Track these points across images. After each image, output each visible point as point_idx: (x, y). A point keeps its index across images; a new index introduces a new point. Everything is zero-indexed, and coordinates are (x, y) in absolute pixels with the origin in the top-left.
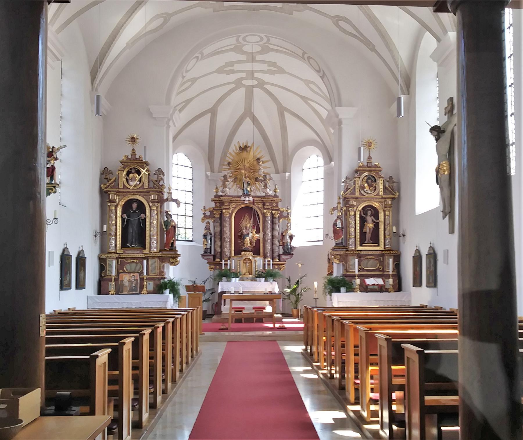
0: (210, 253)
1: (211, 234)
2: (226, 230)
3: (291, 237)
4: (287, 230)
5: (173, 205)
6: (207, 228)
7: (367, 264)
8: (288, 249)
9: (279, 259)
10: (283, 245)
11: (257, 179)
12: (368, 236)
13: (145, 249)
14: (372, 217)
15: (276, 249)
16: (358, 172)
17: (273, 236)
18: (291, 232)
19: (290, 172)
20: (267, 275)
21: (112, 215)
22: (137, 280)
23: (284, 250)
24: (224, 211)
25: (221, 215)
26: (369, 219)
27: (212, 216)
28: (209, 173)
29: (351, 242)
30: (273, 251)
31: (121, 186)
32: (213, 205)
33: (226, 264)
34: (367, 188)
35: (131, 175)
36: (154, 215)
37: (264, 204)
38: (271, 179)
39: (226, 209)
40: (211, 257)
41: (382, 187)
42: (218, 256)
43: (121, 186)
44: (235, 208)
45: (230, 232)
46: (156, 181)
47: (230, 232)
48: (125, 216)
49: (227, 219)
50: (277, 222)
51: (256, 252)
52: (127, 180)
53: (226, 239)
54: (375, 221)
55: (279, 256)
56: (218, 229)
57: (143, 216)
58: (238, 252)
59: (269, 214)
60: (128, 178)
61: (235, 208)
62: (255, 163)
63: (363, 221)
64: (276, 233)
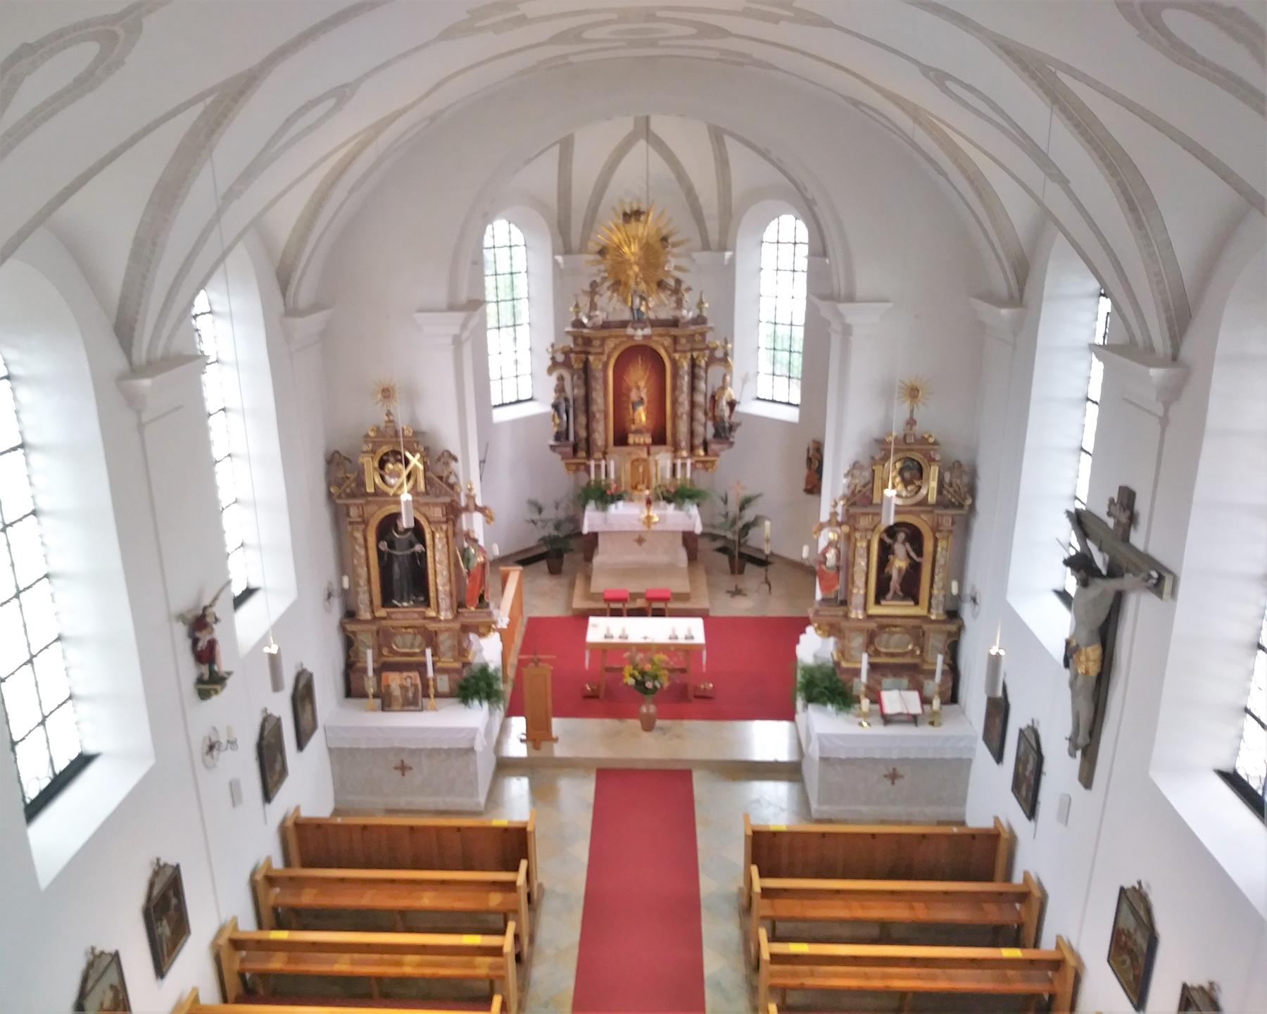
0: (567, 438)
1: (566, 400)
2: (597, 396)
3: (732, 404)
4: (723, 388)
5: (478, 518)
6: (560, 389)
8: (724, 428)
9: (706, 450)
10: (714, 418)
11: (661, 285)
12: (895, 583)
13: (428, 605)
14: (908, 545)
15: (699, 429)
16: (881, 449)
17: (693, 404)
18: (732, 392)
19: (734, 249)
20: (678, 495)
21: (357, 548)
22: (415, 686)
23: (716, 430)
24: (591, 358)
25: (586, 363)
27: (567, 364)
28: (560, 259)
29: (858, 592)
30: (692, 433)
31: (370, 489)
32: (569, 342)
33: (598, 467)
37: (675, 340)
38: (689, 289)
39: (596, 354)
40: (569, 450)
41: (934, 484)
42: (583, 445)
43: (370, 489)
45: (603, 401)
47: (603, 401)
48: (384, 546)
49: (599, 375)
50: (702, 373)
51: (659, 439)
52: (383, 478)
54: (913, 555)
55: (705, 445)
56: (580, 392)
58: (621, 439)
59: (685, 365)
61: (615, 348)
62: (658, 246)
63: (886, 552)
64: (700, 398)
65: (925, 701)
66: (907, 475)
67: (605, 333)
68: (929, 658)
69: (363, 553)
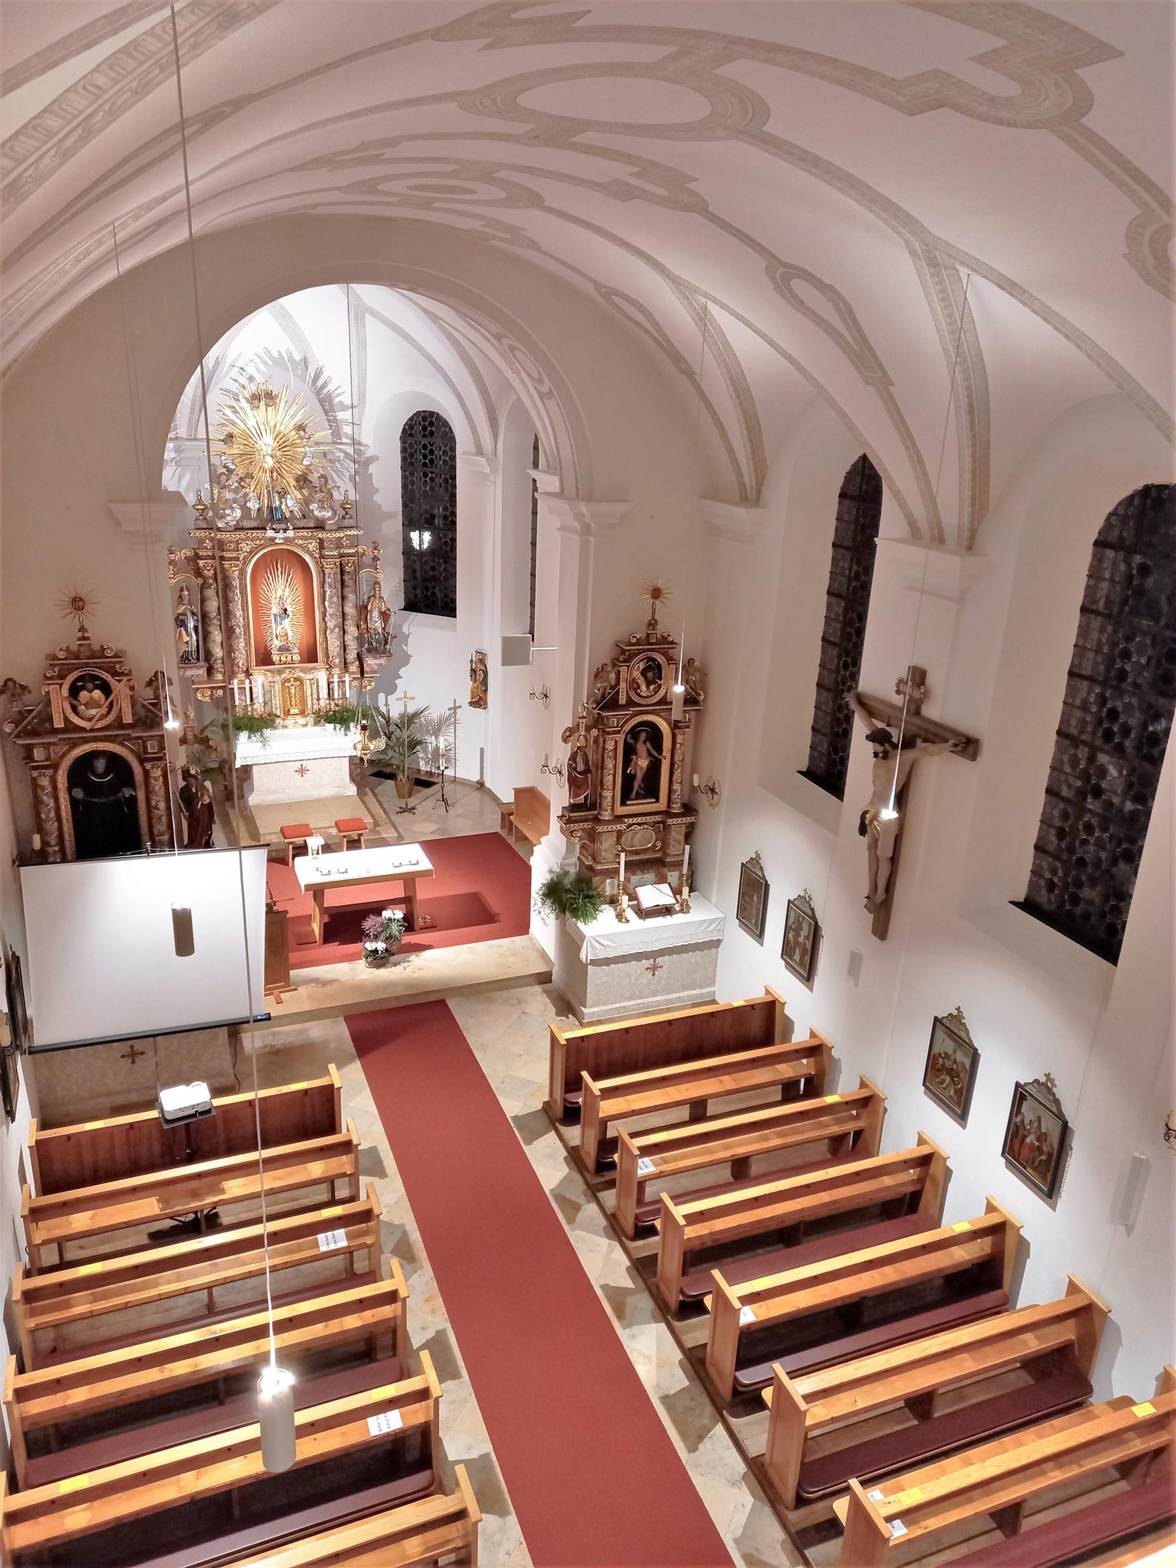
0: (198, 659)
7: (632, 839)
12: (637, 784)
24: (226, 564)
26: (642, 748)
33: (242, 689)
34: (644, 688)
35: (84, 695)
36: (157, 788)
37: (321, 545)
39: (231, 559)
43: (59, 724)
44: (252, 553)
46: (153, 704)
48: (79, 793)
49: (236, 583)
51: (311, 656)
52: (74, 709)
53: (238, 631)
54: (654, 753)
57: (127, 792)
60: (75, 702)
61: (252, 553)
63: (630, 752)
64: (350, 610)
65: (677, 892)
66: (650, 675)
67: (242, 535)
68: (672, 850)
69: (52, 803)
